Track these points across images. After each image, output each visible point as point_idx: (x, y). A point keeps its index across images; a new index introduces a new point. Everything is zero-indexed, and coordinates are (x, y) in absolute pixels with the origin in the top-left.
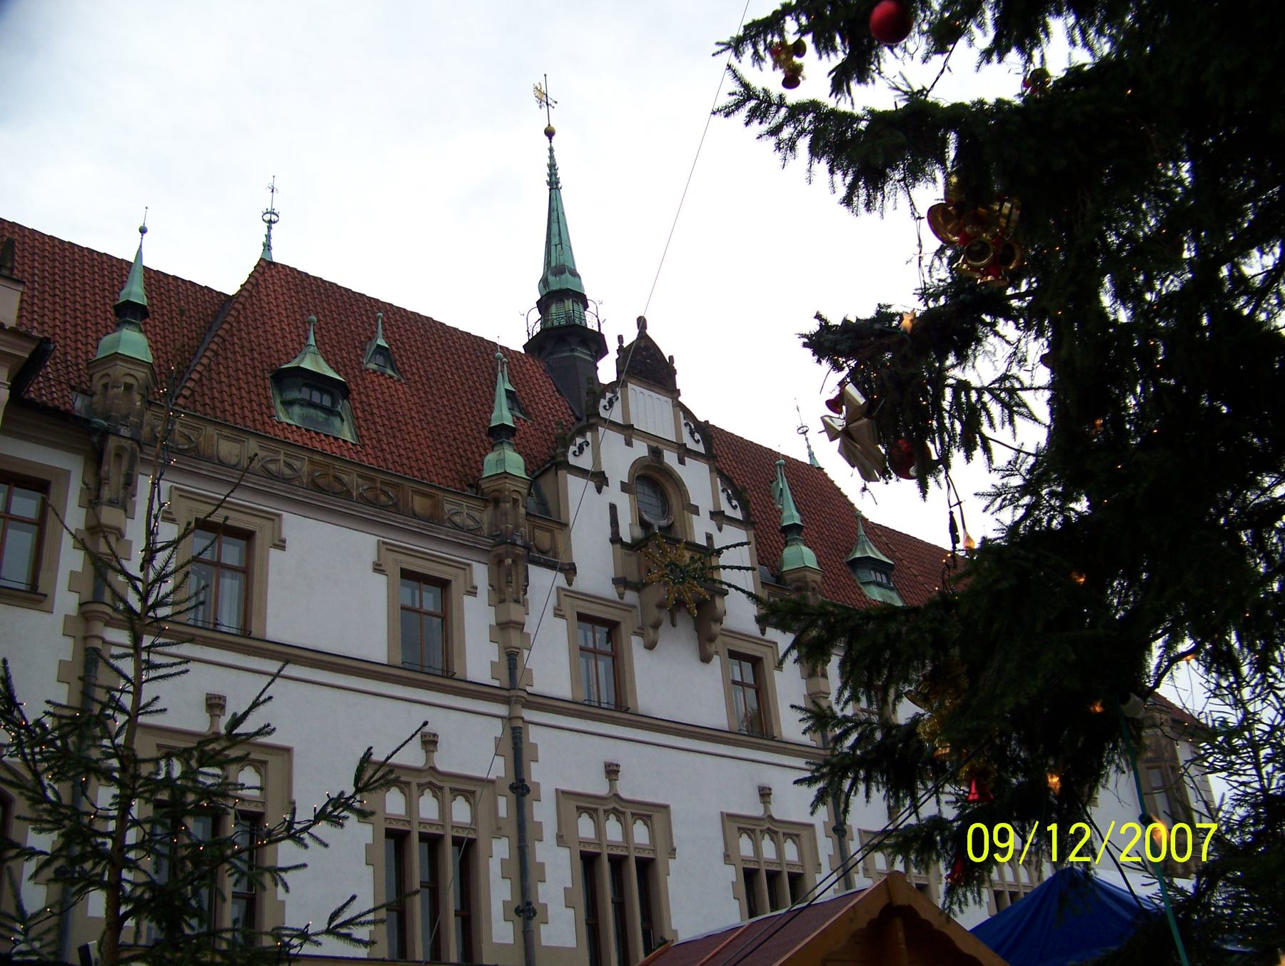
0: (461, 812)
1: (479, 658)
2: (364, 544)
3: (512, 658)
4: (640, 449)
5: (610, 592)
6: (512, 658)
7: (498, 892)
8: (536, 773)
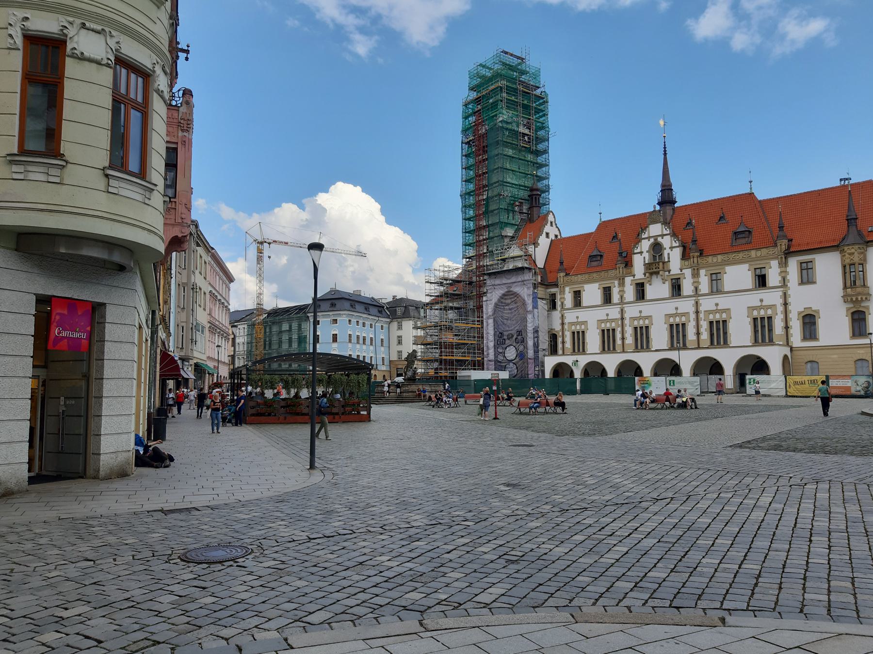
0: (613, 324)
1: (616, 298)
2: (596, 285)
3: (622, 297)
4: (652, 240)
5: (643, 276)
6: (622, 297)
7: (618, 336)
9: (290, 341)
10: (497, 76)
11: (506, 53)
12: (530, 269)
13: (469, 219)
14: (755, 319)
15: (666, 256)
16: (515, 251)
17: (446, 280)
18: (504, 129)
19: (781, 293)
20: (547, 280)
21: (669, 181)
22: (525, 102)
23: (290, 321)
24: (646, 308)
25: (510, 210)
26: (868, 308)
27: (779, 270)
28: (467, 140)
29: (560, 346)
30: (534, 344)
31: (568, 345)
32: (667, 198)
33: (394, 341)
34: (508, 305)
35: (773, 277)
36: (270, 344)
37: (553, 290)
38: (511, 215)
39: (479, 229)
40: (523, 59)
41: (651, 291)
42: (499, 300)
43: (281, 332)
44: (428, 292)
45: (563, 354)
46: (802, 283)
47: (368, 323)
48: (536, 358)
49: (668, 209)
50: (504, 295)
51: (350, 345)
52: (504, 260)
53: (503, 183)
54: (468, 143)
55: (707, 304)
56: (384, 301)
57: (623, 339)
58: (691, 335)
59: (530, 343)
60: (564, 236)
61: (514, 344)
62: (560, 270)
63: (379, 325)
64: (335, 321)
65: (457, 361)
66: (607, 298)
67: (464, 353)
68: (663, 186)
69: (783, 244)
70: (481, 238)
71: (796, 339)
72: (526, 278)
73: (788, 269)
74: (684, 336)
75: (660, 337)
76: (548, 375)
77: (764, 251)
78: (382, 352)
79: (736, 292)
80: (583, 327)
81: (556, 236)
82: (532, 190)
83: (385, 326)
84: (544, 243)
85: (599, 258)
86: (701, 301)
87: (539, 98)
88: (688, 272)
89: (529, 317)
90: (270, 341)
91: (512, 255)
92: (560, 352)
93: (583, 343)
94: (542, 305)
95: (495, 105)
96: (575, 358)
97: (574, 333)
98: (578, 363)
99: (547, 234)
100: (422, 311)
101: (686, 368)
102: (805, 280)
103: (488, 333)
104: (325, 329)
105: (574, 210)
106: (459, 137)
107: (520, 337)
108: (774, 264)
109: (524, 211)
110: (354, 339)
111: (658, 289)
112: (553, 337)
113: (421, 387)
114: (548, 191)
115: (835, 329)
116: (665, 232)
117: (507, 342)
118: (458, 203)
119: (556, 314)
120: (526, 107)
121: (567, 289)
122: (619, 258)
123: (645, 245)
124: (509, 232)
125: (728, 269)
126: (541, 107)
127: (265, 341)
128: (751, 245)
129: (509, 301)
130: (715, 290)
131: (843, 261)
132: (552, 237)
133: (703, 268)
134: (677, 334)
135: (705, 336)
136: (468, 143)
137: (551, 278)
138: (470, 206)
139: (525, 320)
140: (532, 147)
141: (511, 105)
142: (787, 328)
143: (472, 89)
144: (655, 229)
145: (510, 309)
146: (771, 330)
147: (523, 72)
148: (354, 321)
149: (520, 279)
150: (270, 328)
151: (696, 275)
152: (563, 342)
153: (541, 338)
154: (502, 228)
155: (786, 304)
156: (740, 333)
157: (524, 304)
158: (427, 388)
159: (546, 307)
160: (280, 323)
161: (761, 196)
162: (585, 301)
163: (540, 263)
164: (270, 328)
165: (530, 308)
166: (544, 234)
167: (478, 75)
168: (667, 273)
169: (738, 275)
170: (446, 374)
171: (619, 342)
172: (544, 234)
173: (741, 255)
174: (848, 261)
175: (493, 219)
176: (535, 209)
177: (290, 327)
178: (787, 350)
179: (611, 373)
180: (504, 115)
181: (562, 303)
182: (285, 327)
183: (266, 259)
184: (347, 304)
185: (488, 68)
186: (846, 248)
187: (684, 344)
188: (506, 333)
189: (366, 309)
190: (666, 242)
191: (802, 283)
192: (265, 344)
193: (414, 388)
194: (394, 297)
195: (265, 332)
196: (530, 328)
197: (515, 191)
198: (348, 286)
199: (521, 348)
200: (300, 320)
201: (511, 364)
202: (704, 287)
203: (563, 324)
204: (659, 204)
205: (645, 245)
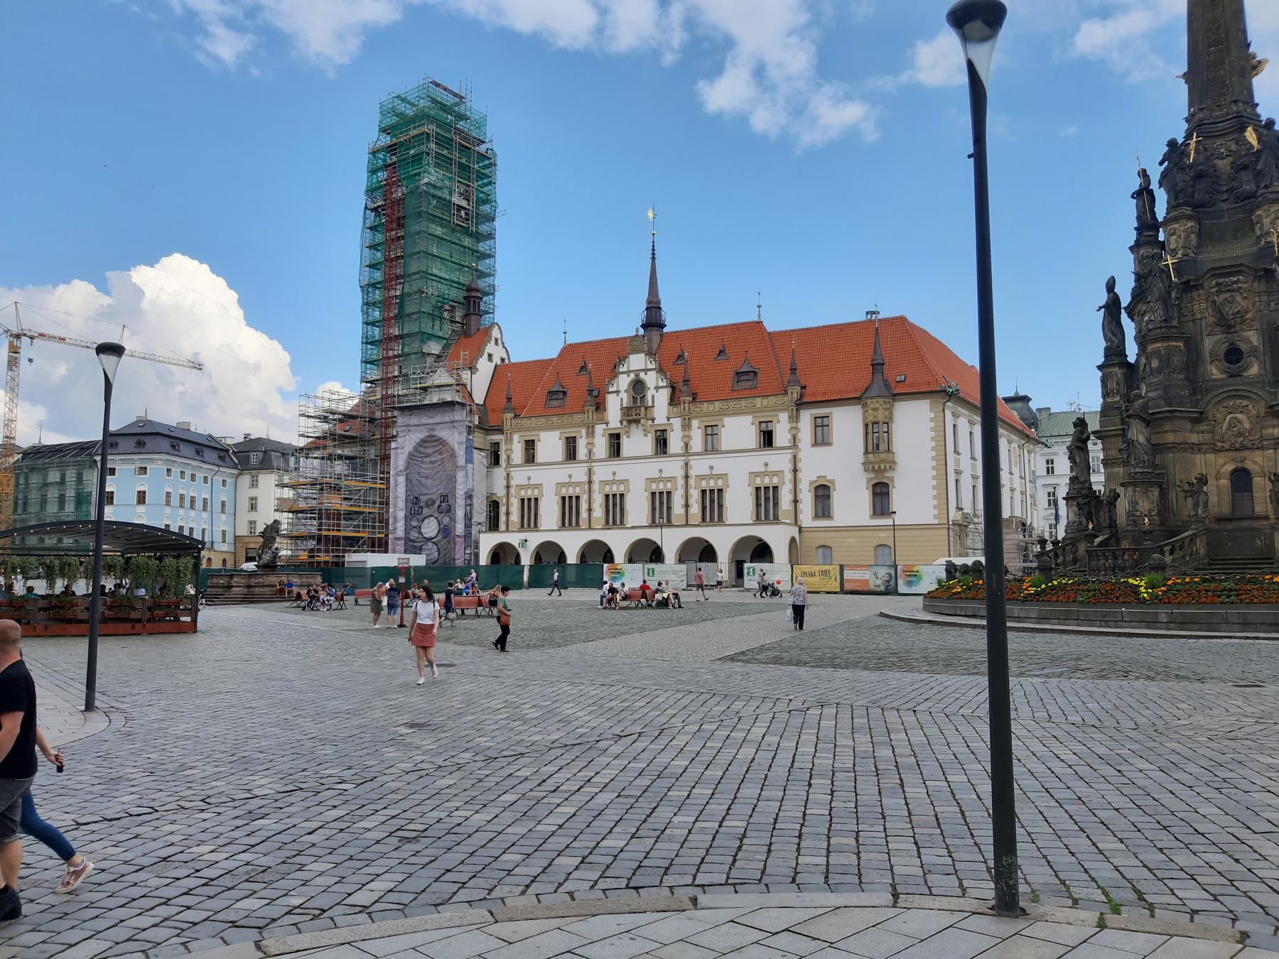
1: (582, 452)
2: (556, 434)
4: (632, 376)
7: (584, 506)
8: (594, 478)
9: (62, 500)
10: (423, 117)
11: (437, 85)
12: (463, 405)
13: (373, 324)
14: (758, 489)
15: (649, 398)
16: (442, 377)
17: (333, 413)
18: (428, 194)
19: (790, 456)
20: (487, 423)
21: (657, 296)
22: (463, 161)
23: (62, 467)
24: (620, 469)
25: (436, 315)
26: (892, 479)
27: (788, 426)
28: (373, 206)
29: (502, 518)
30: (466, 515)
31: (515, 517)
32: (653, 321)
33: (244, 504)
34: (428, 456)
35: (782, 436)
36: (25, 504)
37: (496, 437)
38: (437, 322)
39: (388, 340)
40: (461, 98)
41: (627, 446)
42: (415, 449)
43: (46, 485)
44: (302, 430)
45: (507, 530)
46: (816, 444)
47: (200, 476)
48: (468, 535)
49: (655, 335)
50: (423, 441)
51: (168, 510)
52: (425, 389)
53: (426, 275)
54: (375, 210)
55: (700, 466)
56: (229, 442)
57: (590, 510)
58: (678, 508)
59: (460, 513)
60: (513, 361)
61: (436, 514)
62: (506, 410)
63: (219, 479)
64: (143, 470)
65: (345, 538)
66: (571, 454)
67: (358, 526)
68: (649, 302)
69: (795, 391)
70: (391, 353)
71: (807, 518)
72: (456, 418)
73: (800, 425)
74: (669, 508)
75: (638, 509)
76: (484, 560)
77: (772, 400)
78: (223, 522)
79: (735, 452)
80: (536, 492)
81: (503, 360)
82: (469, 289)
83: (230, 481)
84: (485, 368)
85: (561, 396)
86: (692, 463)
87: (483, 157)
88: (677, 423)
89: (460, 475)
90: (26, 499)
91: (437, 382)
92: (502, 527)
93: (536, 515)
94: (480, 458)
95: (418, 159)
96: (523, 536)
97: (523, 500)
98: (527, 544)
99: (490, 356)
100: (292, 460)
101: (670, 553)
102: (819, 440)
103: (396, 497)
104: (123, 483)
105: (527, 326)
106: (361, 200)
107: (445, 505)
108: (784, 417)
109: (457, 319)
110: (175, 500)
111: (637, 443)
112: (494, 506)
113: (284, 579)
114: (493, 294)
115: (852, 505)
116: (650, 366)
117: (426, 511)
118: (357, 298)
119: (499, 472)
120: (464, 168)
121: (516, 437)
122: (589, 398)
123: (623, 382)
124: (434, 348)
125: (728, 421)
126: (487, 171)
127: (16, 499)
128: (754, 392)
129: (430, 451)
130: (710, 448)
131: (865, 418)
132: (497, 360)
133: (696, 417)
134: (660, 503)
135: (695, 509)
136: (375, 210)
137: (492, 420)
138: (374, 304)
139: (452, 479)
140: (472, 226)
141: (443, 162)
142: (796, 501)
143: (383, 130)
144: (637, 361)
145: (432, 463)
146: (776, 504)
147: (462, 117)
148: (176, 471)
149: (447, 419)
150: (27, 479)
151: (686, 426)
152: (508, 514)
153: (475, 507)
154: (422, 342)
155: (795, 471)
156: (739, 505)
157: (453, 455)
158: (295, 580)
159: (485, 462)
160: (44, 470)
161: (771, 327)
162: (541, 456)
163: (479, 398)
164: (27, 479)
165: (461, 462)
166: (486, 355)
167: (394, 112)
168: (650, 422)
169: (739, 429)
170: (327, 559)
171: (584, 514)
172: (486, 355)
173: (743, 403)
174: (870, 419)
175: (410, 327)
176: (473, 318)
177: (63, 477)
178: (794, 532)
179: (572, 558)
180: (431, 175)
181: (508, 457)
182: (54, 476)
183: (23, 363)
184: (165, 444)
185: (410, 103)
186: (869, 401)
187: (669, 520)
188: (423, 498)
189: (197, 452)
190: (651, 379)
191: (816, 444)
192: (16, 504)
193: (273, 579)
194: (246, 436)
195: (17, 484)
196: (460, 491)
197: (445, 289)
198: (168, 414)
199: (446, 520)
200: (81, 467)
201: (430, 544)
202: (697, 443)
203: (508, 487)
204: (644, 326)
205: (623, 382)
